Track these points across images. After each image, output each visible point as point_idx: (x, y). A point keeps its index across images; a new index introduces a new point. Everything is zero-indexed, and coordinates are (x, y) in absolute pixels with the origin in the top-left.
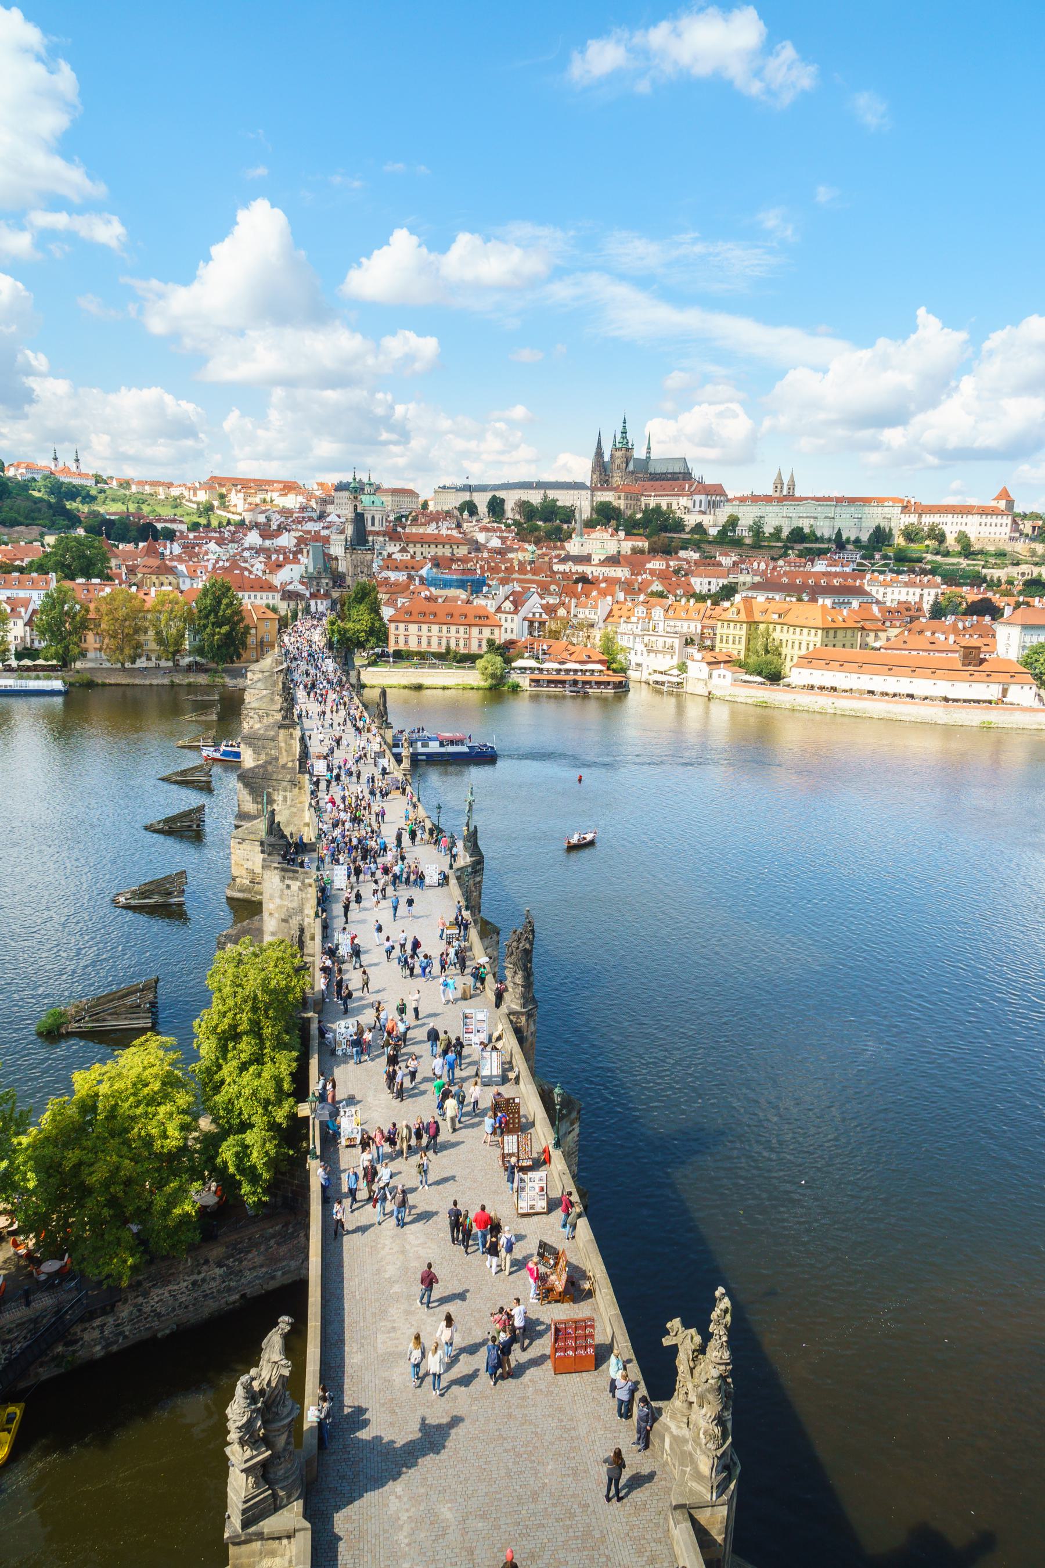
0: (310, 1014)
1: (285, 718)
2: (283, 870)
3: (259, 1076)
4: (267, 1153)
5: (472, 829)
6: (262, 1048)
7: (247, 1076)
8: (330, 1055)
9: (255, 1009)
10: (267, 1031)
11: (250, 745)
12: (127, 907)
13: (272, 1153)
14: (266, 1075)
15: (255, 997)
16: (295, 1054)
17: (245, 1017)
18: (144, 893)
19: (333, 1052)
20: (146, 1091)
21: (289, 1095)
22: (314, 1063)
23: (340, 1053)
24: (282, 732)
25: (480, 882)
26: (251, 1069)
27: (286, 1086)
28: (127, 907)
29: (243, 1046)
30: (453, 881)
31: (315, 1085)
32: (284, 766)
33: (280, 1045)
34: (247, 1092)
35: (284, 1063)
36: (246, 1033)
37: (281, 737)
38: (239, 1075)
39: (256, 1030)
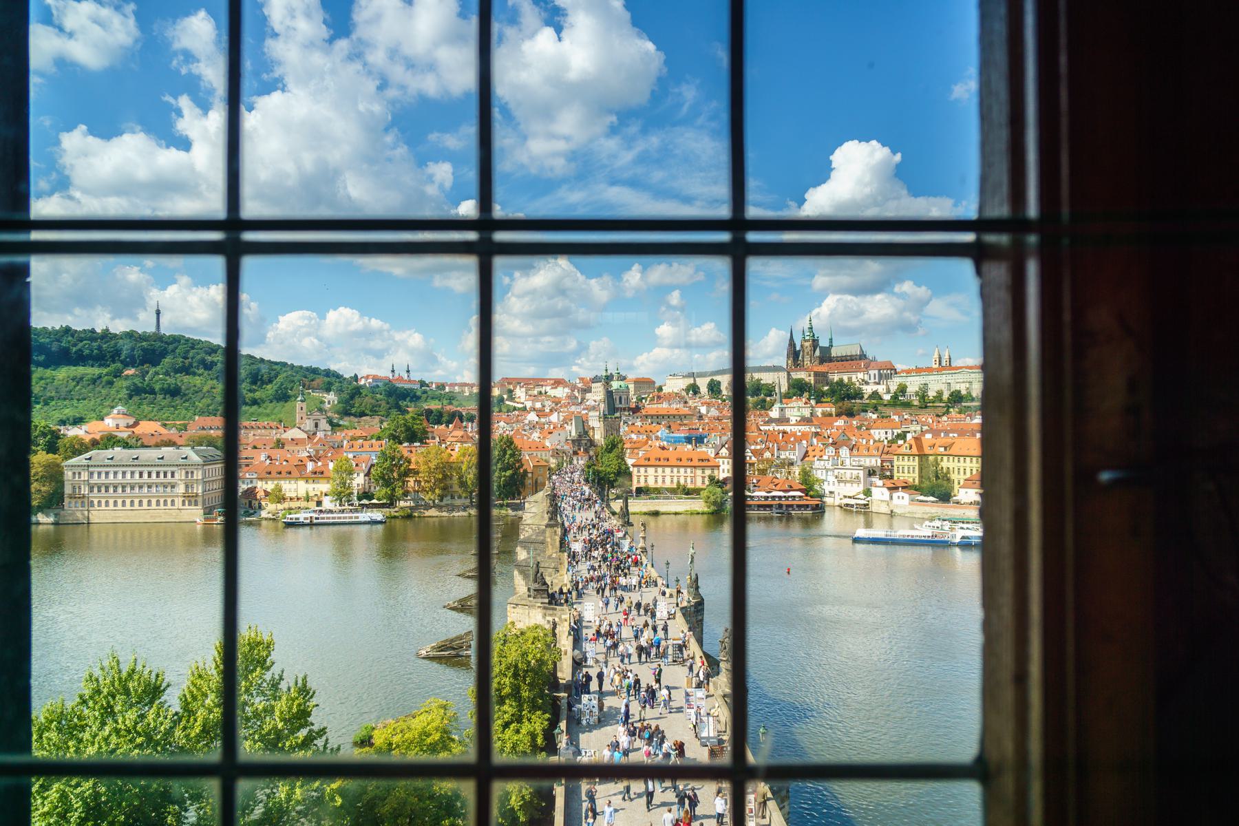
0: (562, 694)
1: (551, 519)
2: (545, 608)
3: (518, 732)
4: (523, 797)
5: (694, 577)
6: (521, 710)
7: (509, 732)
8: (575, 725)
9: (515, 675)
10: (525, 694)
11: (525, 548)
12: (427, 658)
13: (527, 797)
14: (523, 731)
15: (516, 666)
16: (547, 716)
17: (507, 681)
18: (442, 648)
19: (579, 722)
20: (429, 740)
21: (542, 750)
22: (563, 725)
23: (584, 722)
24: (548, 530)
25: (702, 620)
26: (512, 726)
27: (539, 741)
28: (427, 658)
29: (506, 708)
30: (679, 615)
31: (563, 741)
32: (550, 557)
33: (534, 708)
34: (509, 745)
35: (537, 723)
36: (508, 696)
37: (548, 534)
38: (503, 732)
39: (516, 694)
